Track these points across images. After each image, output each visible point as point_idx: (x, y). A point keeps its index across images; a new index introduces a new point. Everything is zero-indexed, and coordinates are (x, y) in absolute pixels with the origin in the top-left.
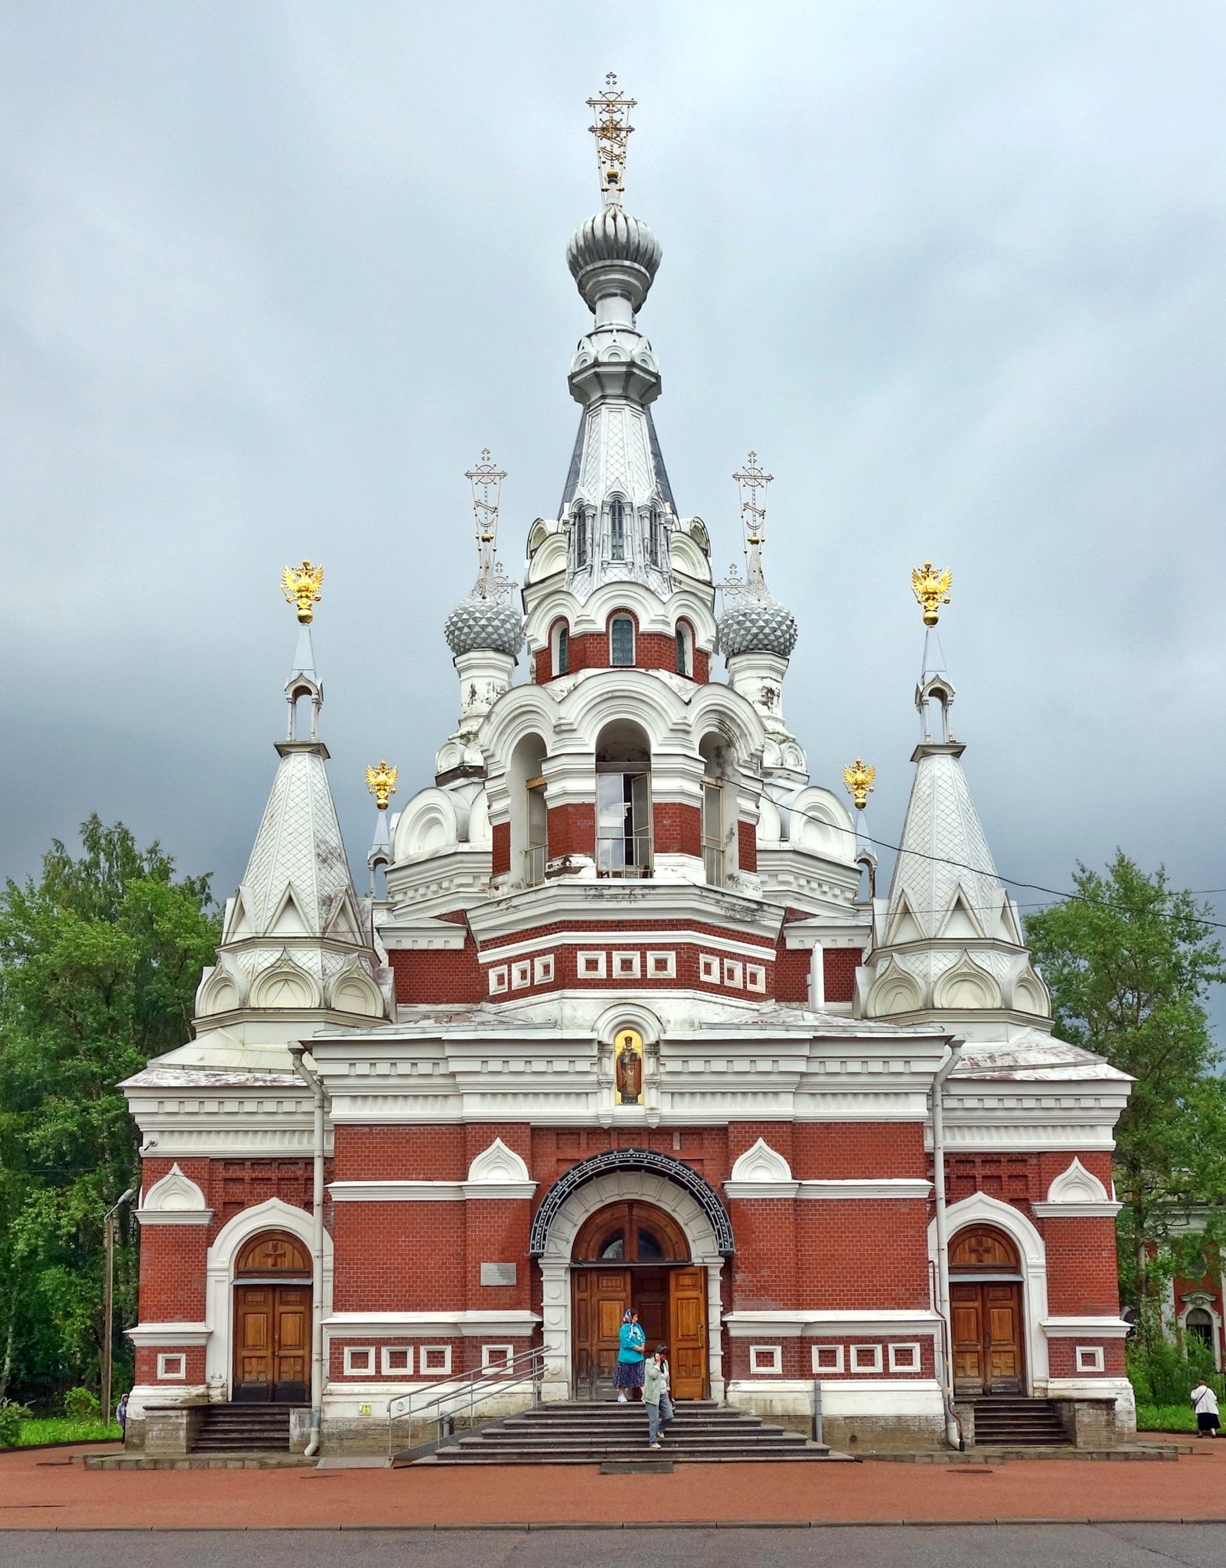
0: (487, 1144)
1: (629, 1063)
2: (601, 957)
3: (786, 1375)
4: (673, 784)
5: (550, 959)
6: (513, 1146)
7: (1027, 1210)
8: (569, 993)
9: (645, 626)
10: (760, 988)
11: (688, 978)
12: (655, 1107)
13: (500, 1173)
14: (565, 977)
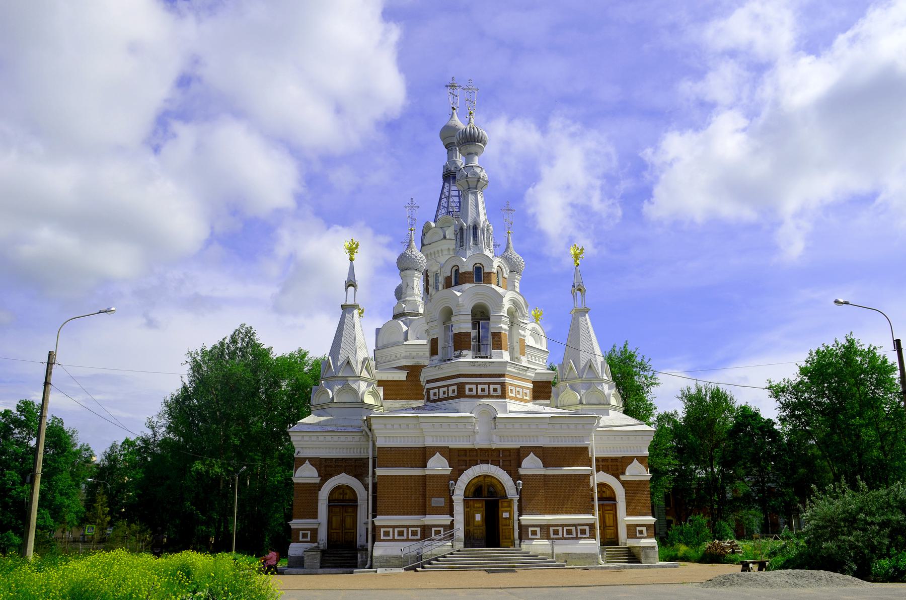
2: (474, 387)
3: (541, 538)
5: (455, 387)
7: (618, 478)
8: (462, 399)
10: (527, 398)
13: (438, 466)
14: (461, 393)
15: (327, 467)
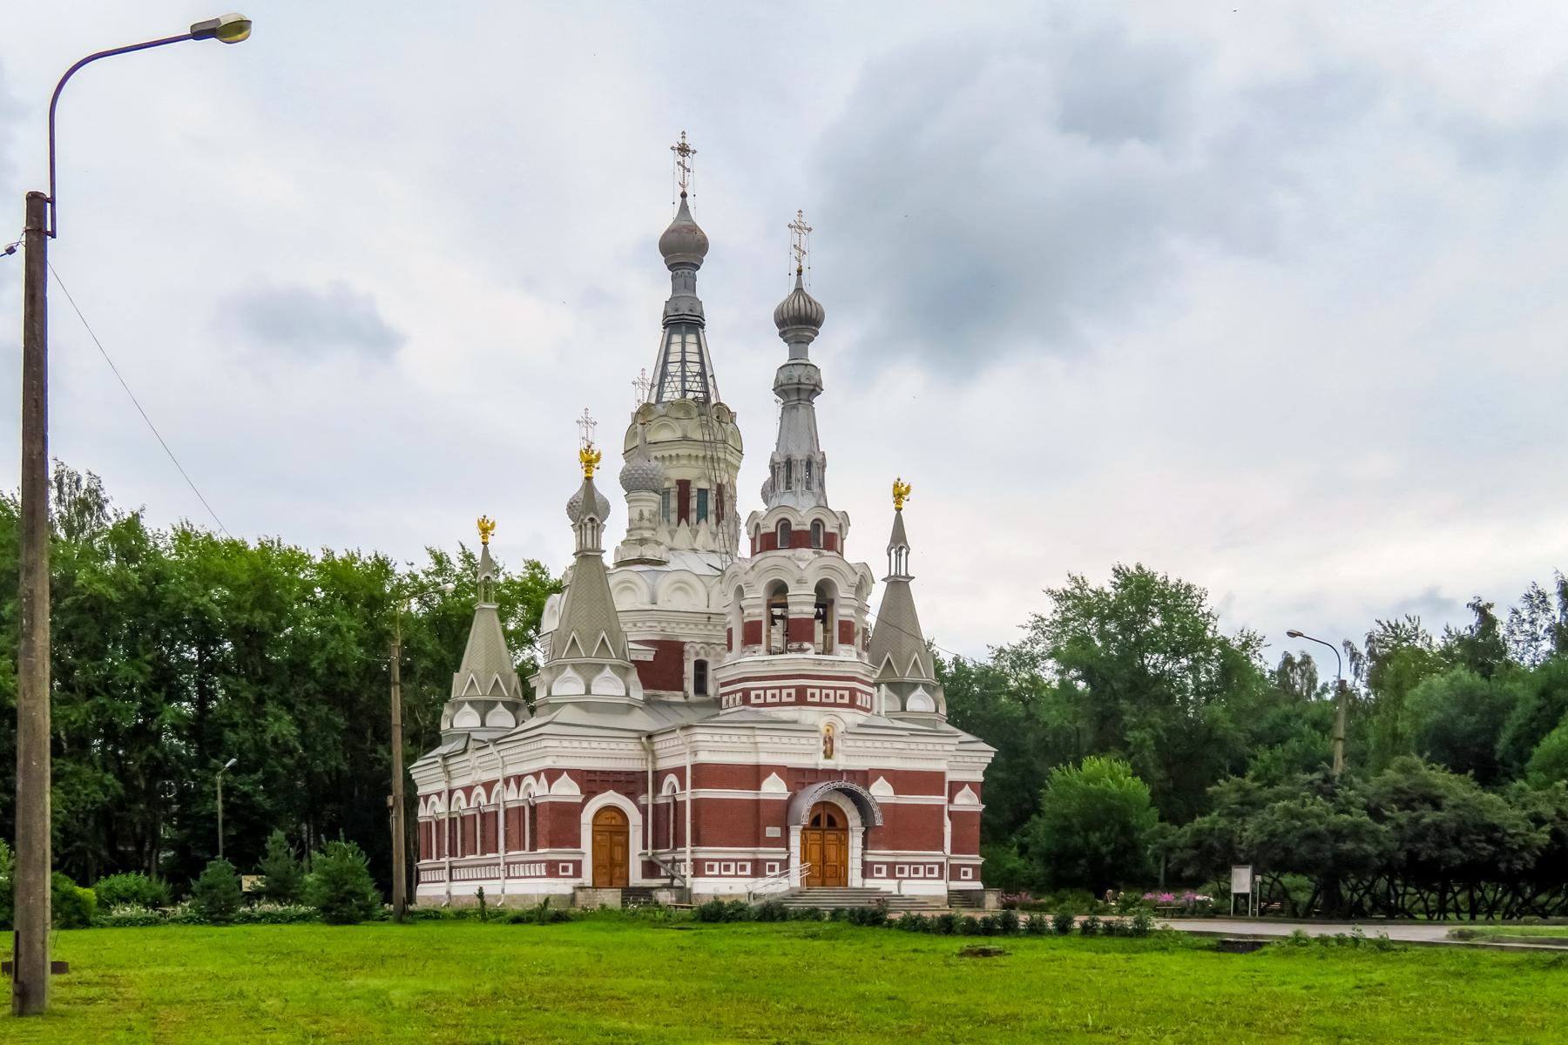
0: (768, 775)
1: (829, 741)
2: (817, 692)
4: (842, 612)
5: (793, 691)
6: (780, 775)
9: (829, 529)
11: (852, 704)
12: (840, 762)
13: (774, 788)
14: (801, 699)
15: (592, 782)
